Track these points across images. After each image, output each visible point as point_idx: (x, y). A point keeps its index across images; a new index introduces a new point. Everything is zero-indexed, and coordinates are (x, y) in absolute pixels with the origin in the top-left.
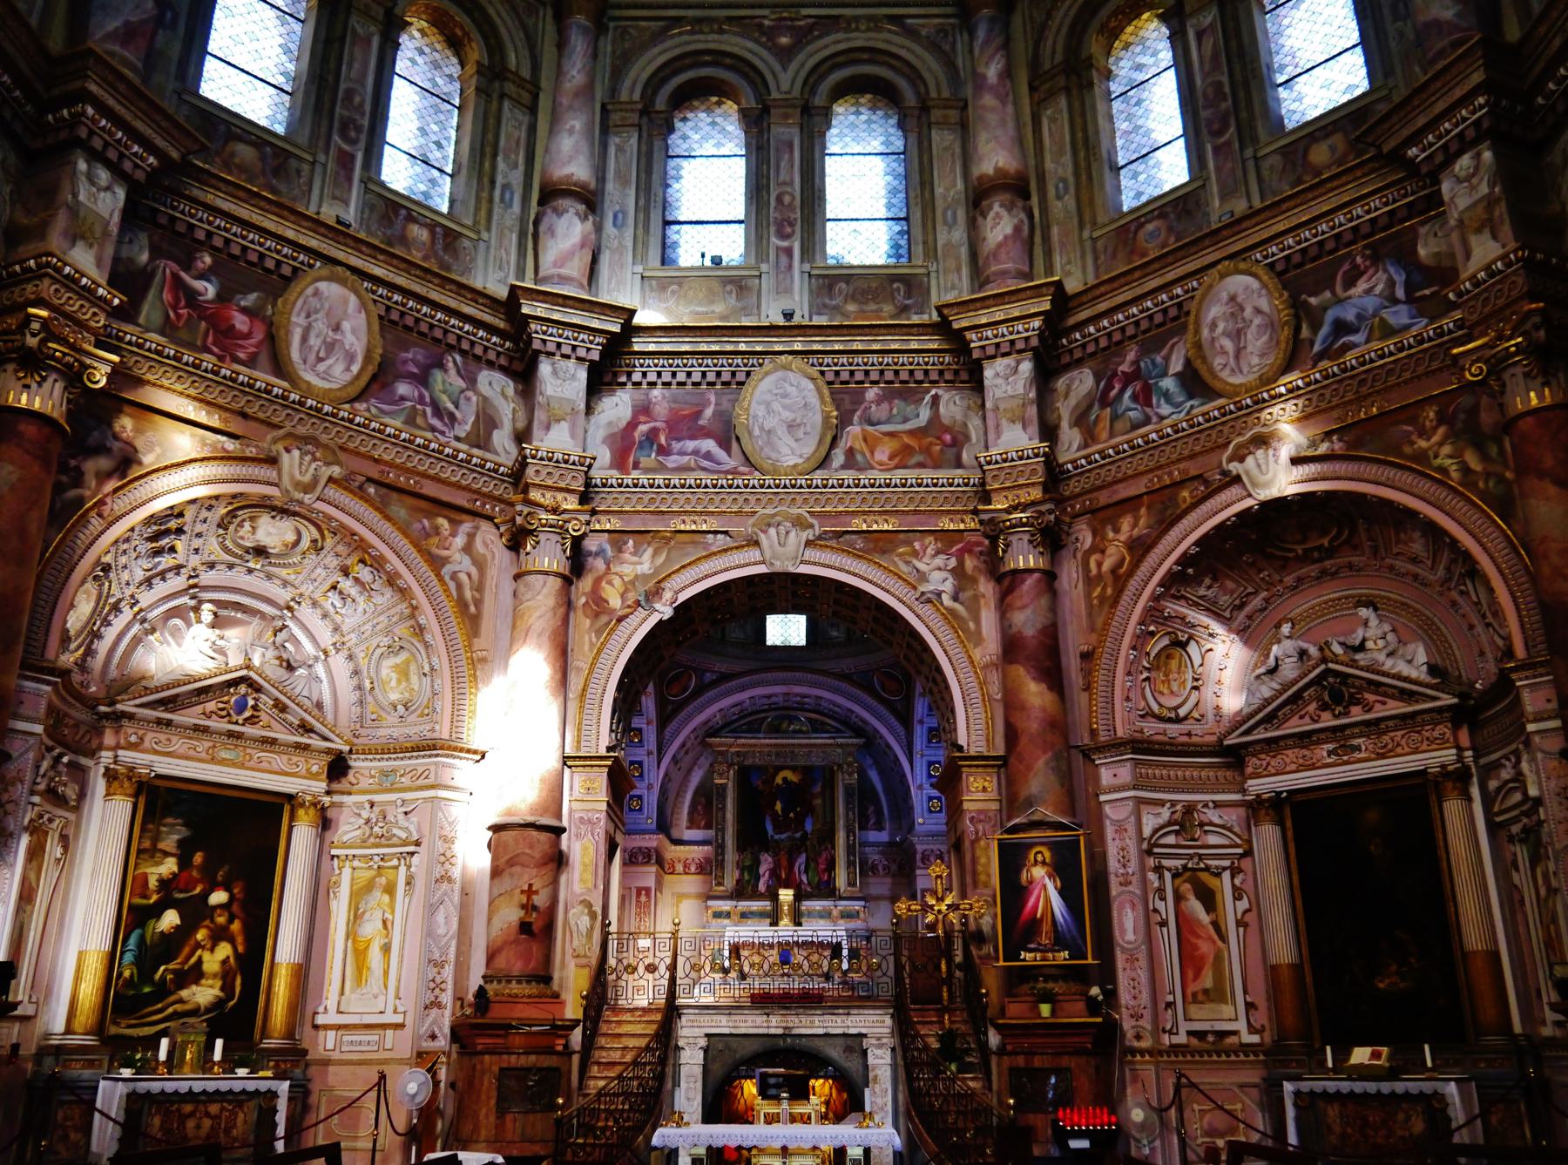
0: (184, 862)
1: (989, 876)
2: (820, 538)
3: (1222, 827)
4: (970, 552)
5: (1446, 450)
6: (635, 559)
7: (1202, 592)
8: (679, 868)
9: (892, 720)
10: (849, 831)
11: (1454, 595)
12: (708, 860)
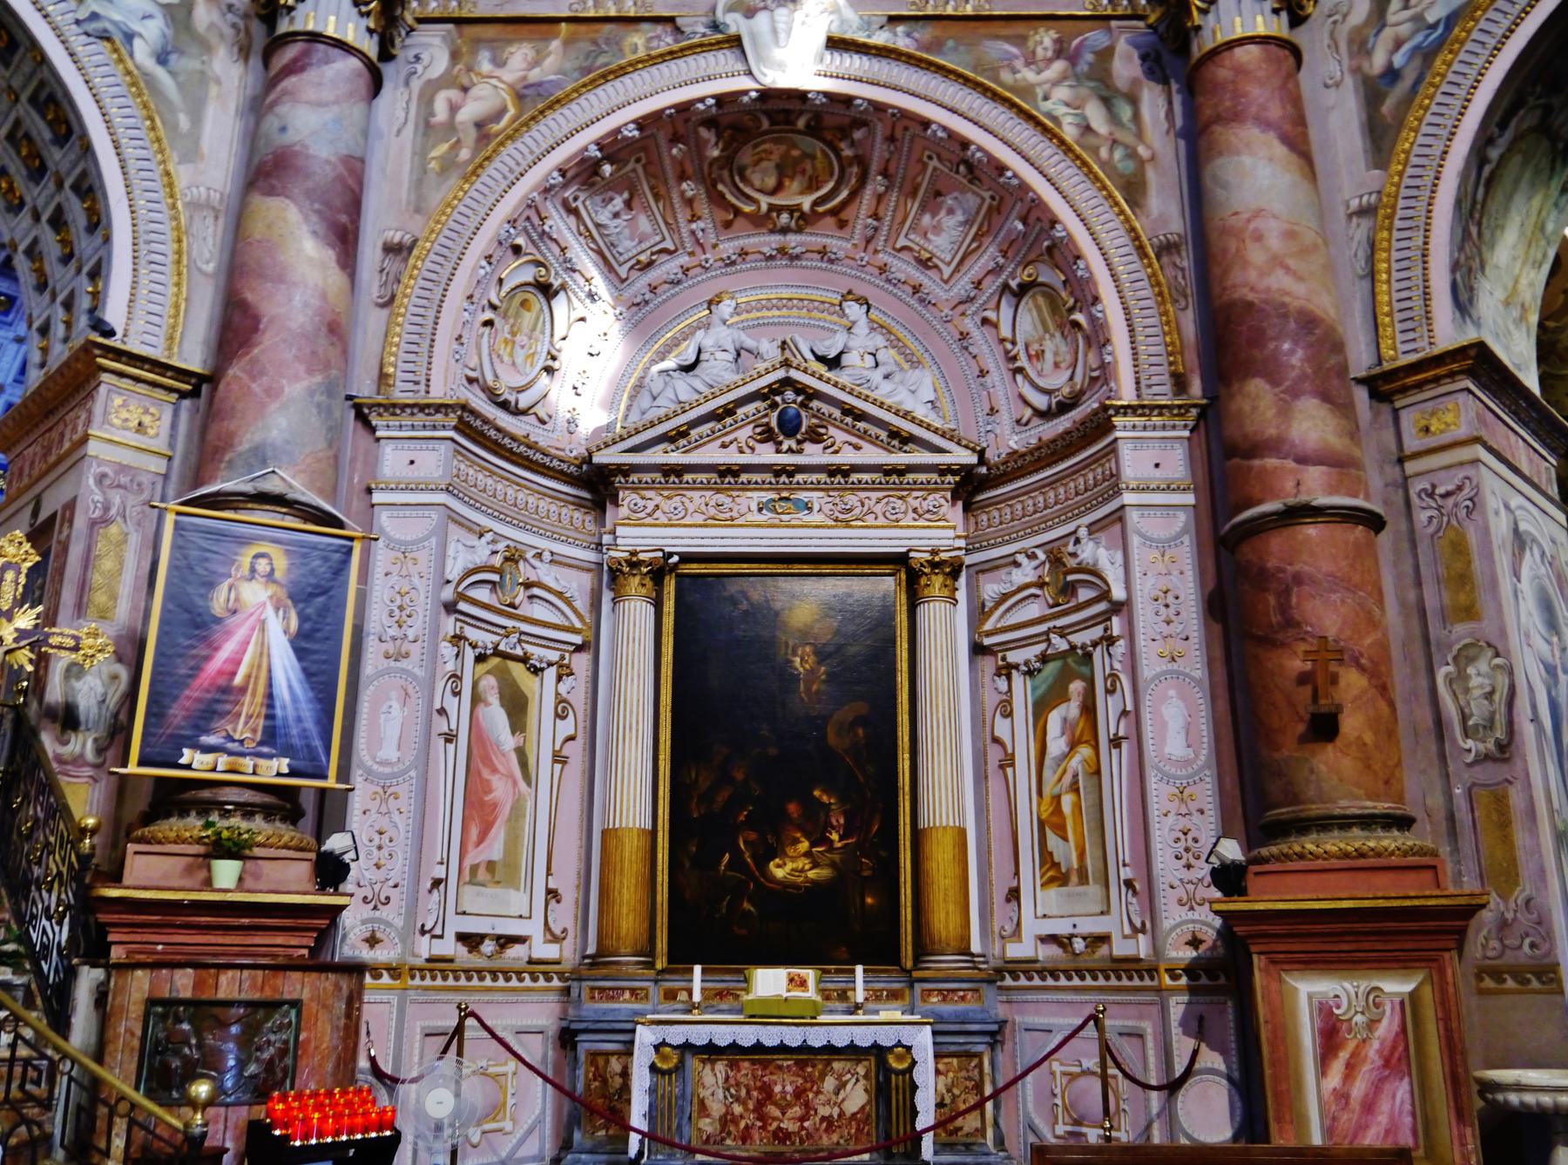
1: (114, 597)
3: (560, 595)
5: (1062, 93)
7: (604, 217)
11: (970, 325)
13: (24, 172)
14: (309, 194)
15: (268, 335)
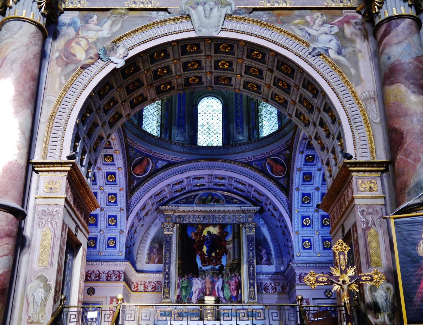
1: (379, 257)
2: (235, 12)
4: (348, 22)
6: (98, 28)
8: (141, 288)
9: (278, 191)
10: (250, 265)
12: (159, 283)
13: (307, 111)
14: (406, 78)
15: (408, 138)
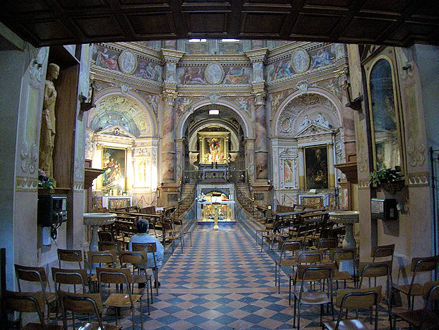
0: (110, 161)
